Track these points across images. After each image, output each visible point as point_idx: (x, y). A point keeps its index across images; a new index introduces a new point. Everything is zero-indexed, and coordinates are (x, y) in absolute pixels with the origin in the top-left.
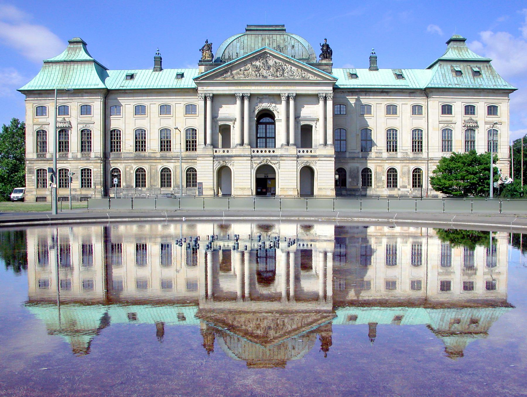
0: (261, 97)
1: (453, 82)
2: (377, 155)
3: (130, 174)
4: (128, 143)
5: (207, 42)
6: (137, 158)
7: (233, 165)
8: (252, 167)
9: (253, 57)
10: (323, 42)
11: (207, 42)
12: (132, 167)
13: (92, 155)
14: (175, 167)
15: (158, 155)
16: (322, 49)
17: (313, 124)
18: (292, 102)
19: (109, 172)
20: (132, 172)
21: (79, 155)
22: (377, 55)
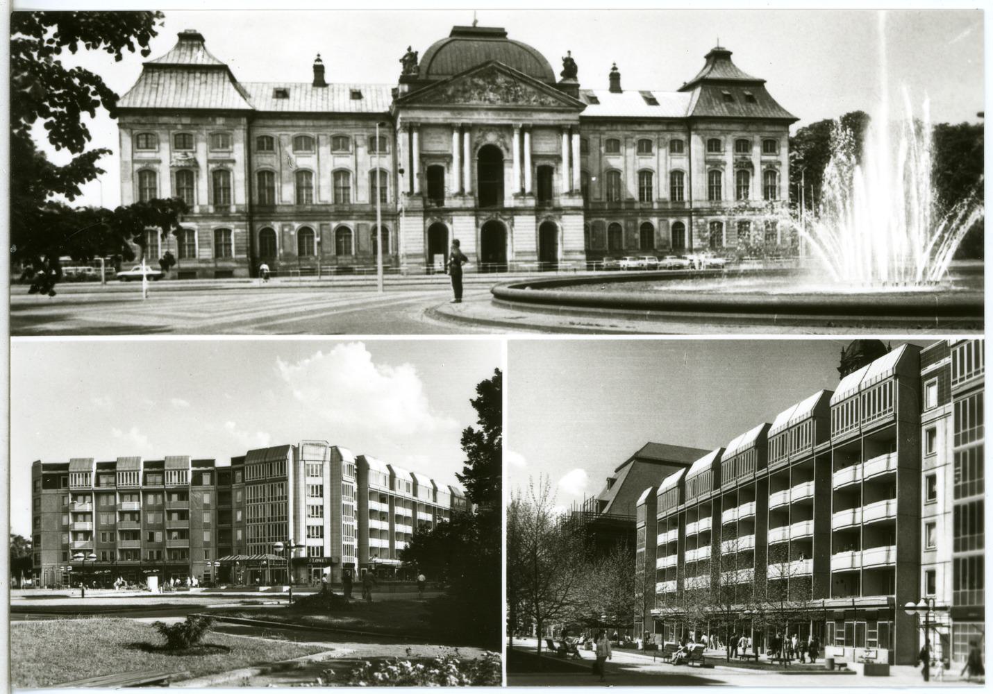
0: (484, 129)
1: (720, 110)
2: (628, 206)
3: (291, 236)
4: (286, 193)
5: (409, 49)
6: (299, 215)
7: (451, 223)
8: (477, 225)
9: (476, 74)
10: (566, 55)
11: (409, 49)
12: (293, 227)
13: (233, 209)
14: (358, 226)
15: (332, 209)
16: (564, 65)
17: (552, 163)
18: (527, 136)
19: (258, 234)
20: (293, 233)
21: (211, 210)
22: (618, 71)
